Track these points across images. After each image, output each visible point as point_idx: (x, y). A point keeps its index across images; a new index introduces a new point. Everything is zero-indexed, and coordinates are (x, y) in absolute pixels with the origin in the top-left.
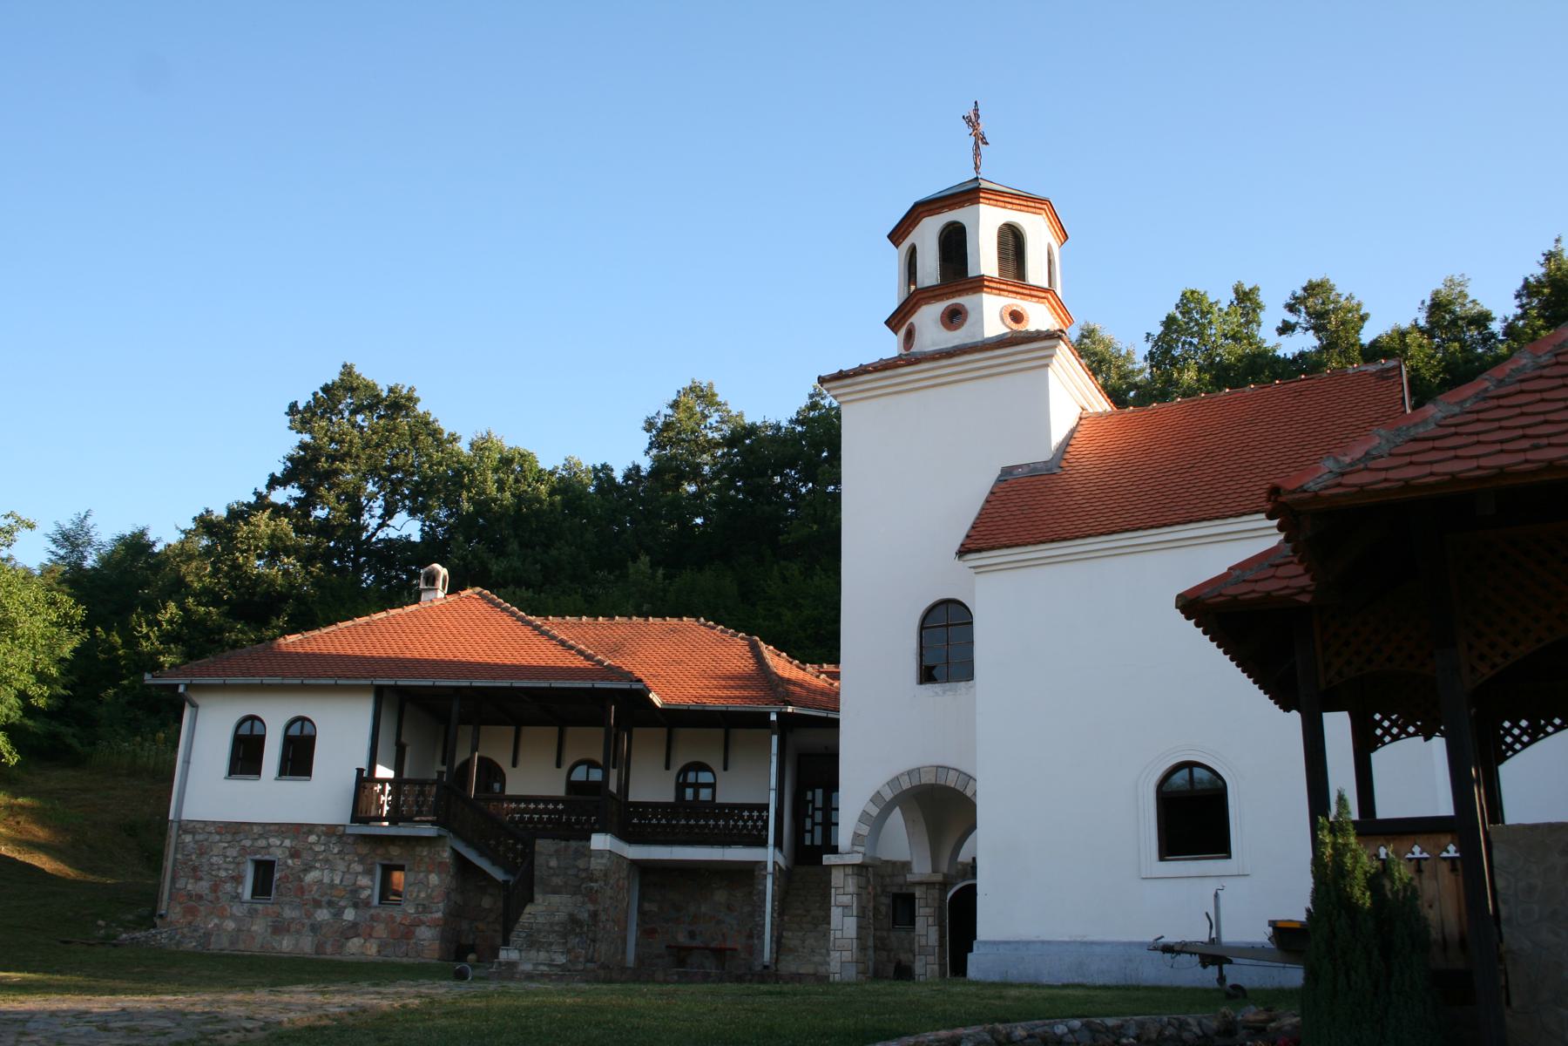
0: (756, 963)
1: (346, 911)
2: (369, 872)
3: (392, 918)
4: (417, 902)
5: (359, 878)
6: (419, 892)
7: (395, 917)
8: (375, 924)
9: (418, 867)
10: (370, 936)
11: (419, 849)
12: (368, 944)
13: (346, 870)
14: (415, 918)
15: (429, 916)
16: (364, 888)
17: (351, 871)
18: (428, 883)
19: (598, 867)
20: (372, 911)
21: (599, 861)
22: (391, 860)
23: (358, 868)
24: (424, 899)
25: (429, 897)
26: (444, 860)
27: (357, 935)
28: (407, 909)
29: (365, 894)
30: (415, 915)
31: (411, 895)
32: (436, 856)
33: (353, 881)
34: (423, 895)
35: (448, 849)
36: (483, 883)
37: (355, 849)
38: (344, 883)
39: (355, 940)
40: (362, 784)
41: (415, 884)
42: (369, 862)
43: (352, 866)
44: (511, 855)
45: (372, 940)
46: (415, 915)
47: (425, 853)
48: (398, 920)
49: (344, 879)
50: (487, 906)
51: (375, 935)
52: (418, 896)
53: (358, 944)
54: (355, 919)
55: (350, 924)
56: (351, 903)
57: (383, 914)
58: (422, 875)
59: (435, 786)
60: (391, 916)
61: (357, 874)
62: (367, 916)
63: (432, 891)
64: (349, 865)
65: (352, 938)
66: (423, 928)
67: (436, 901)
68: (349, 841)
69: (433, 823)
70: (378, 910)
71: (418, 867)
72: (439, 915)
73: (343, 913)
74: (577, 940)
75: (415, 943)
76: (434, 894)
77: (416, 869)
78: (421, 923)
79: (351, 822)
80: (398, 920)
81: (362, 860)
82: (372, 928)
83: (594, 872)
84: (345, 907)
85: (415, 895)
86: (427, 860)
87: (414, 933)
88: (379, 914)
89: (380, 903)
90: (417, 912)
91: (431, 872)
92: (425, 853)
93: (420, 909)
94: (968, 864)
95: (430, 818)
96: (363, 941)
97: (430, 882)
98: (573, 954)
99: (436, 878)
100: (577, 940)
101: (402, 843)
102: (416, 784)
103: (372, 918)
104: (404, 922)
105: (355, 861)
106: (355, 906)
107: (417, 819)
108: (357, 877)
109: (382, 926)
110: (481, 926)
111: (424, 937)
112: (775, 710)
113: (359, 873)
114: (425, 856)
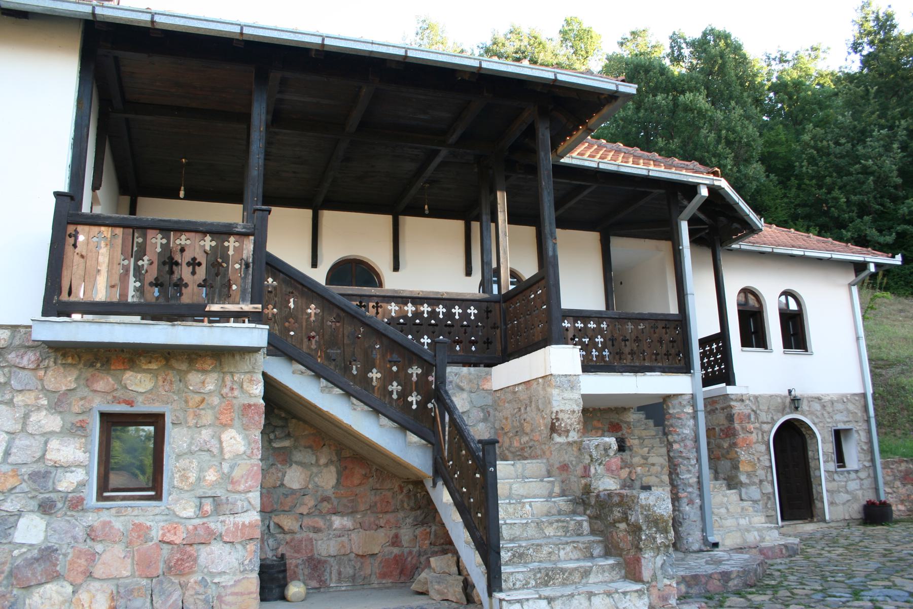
0: (690, 540)
1: (23, 522)
2: (77, 430)
3: (141, 531)
4: (200, 492)
5: (54, 444)
6: (201, 470)
7: (149, 528)
8: (99, 548)
9: (197, 416)
10: (90, 576)
11: (194, 378)
12: (84, 596)
13: (18, 427)
14: (195, 528)
15: (230, 520)
16: (66, 468)
17: (30, 429)
18: (221, 449)
19: (567, 407)
20: (91, 519)
21: (567, 395)
22: (130, 403)
23: (54, 423)
24: (213, 485)
25: (227, 479)
26: (252, 401)
27: (55, 577)
28: (177, 509)
29: (67, 482)
30: (197, 521)
31: (184, 478)
32: (236, 393)
33: (38, 455)
34: (211, 476)
35: (260, 377)
36: (286, 443)
37: (41, 380)
38: (11, 459)
39: (51, 589)
40: (71, 229)
41: (192, 453)
42: (76, 409)
43: (34, 418)
44: (395, 387)
45: (96, 585)
46: (197, 521)
47: (210, 387)
48: (156, 534)
49: (14, 450)
50: (296, 486)
51: (99, 571)
52: (199, 479)
53: (57, 598)
54: (46, 538)
55: (35, 553)
56: (34, 504)
57: (118, 524)
58: (206, 434)
59: (252, 238)
60: (138, 527)
61: (47, 436)
62: (80, 532)
63: (232, 468)
64: (26, 416)
65: (40, 584)
66: (216, 548)
67: (242, 487)
68: (25, 362)
69: (255, 318)
70: (105, 516)
71: (197, 416)
72: (254, 517)
73: (14, 526)
74: (659, 560)
75: (203, 583)
76: (237, 473)
77: (192, 422)
78: (212, 537)
79: (44, 314)
80: (156, 534)
81: (58, 403)
82: (93, 557)
83: (560, 416)
84: (19, 514)
85: (192, 479)
86: (216, 400)
87: (195, 560)
88: (106, 524)
89: (100, 497)
90: (201, 513)
91: (225, 426)
92: (210, 387)
93: (208, 507)
94: (785, 397)
95: (247, 307)
96: (69, 589)
97: (227, 449)
98: (654, 591)
99: (239, 438)
100: (659, 560)
101: (154, 366)
102: (205, 233)
103: (91, 534)
104: (169, 537)
105: (39, 408)
106: (46, 508)
107: (216, 308)
108: (46, 443)
109: (118, 550)
110: (288, 522)
111: (220, 568)
112: (707, 182)
113: (52, 433)
114: (210, 393)
